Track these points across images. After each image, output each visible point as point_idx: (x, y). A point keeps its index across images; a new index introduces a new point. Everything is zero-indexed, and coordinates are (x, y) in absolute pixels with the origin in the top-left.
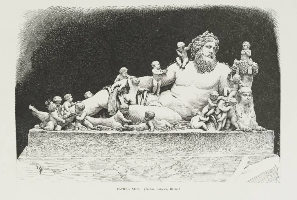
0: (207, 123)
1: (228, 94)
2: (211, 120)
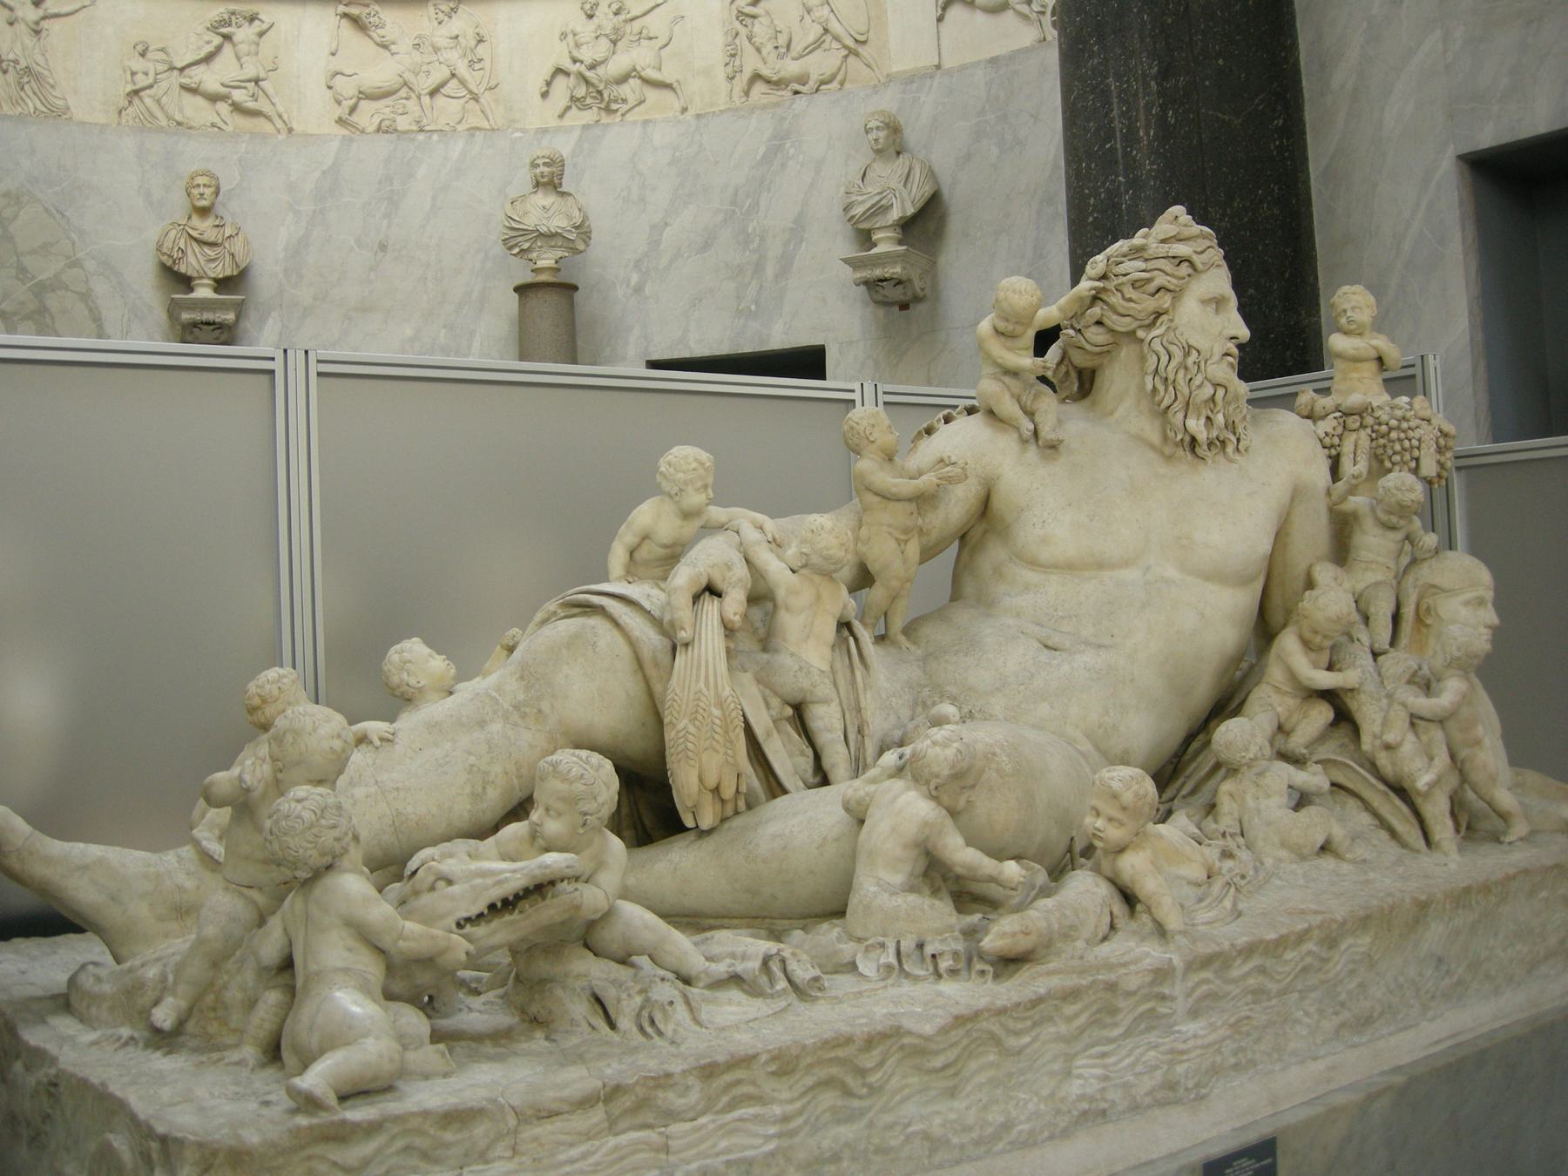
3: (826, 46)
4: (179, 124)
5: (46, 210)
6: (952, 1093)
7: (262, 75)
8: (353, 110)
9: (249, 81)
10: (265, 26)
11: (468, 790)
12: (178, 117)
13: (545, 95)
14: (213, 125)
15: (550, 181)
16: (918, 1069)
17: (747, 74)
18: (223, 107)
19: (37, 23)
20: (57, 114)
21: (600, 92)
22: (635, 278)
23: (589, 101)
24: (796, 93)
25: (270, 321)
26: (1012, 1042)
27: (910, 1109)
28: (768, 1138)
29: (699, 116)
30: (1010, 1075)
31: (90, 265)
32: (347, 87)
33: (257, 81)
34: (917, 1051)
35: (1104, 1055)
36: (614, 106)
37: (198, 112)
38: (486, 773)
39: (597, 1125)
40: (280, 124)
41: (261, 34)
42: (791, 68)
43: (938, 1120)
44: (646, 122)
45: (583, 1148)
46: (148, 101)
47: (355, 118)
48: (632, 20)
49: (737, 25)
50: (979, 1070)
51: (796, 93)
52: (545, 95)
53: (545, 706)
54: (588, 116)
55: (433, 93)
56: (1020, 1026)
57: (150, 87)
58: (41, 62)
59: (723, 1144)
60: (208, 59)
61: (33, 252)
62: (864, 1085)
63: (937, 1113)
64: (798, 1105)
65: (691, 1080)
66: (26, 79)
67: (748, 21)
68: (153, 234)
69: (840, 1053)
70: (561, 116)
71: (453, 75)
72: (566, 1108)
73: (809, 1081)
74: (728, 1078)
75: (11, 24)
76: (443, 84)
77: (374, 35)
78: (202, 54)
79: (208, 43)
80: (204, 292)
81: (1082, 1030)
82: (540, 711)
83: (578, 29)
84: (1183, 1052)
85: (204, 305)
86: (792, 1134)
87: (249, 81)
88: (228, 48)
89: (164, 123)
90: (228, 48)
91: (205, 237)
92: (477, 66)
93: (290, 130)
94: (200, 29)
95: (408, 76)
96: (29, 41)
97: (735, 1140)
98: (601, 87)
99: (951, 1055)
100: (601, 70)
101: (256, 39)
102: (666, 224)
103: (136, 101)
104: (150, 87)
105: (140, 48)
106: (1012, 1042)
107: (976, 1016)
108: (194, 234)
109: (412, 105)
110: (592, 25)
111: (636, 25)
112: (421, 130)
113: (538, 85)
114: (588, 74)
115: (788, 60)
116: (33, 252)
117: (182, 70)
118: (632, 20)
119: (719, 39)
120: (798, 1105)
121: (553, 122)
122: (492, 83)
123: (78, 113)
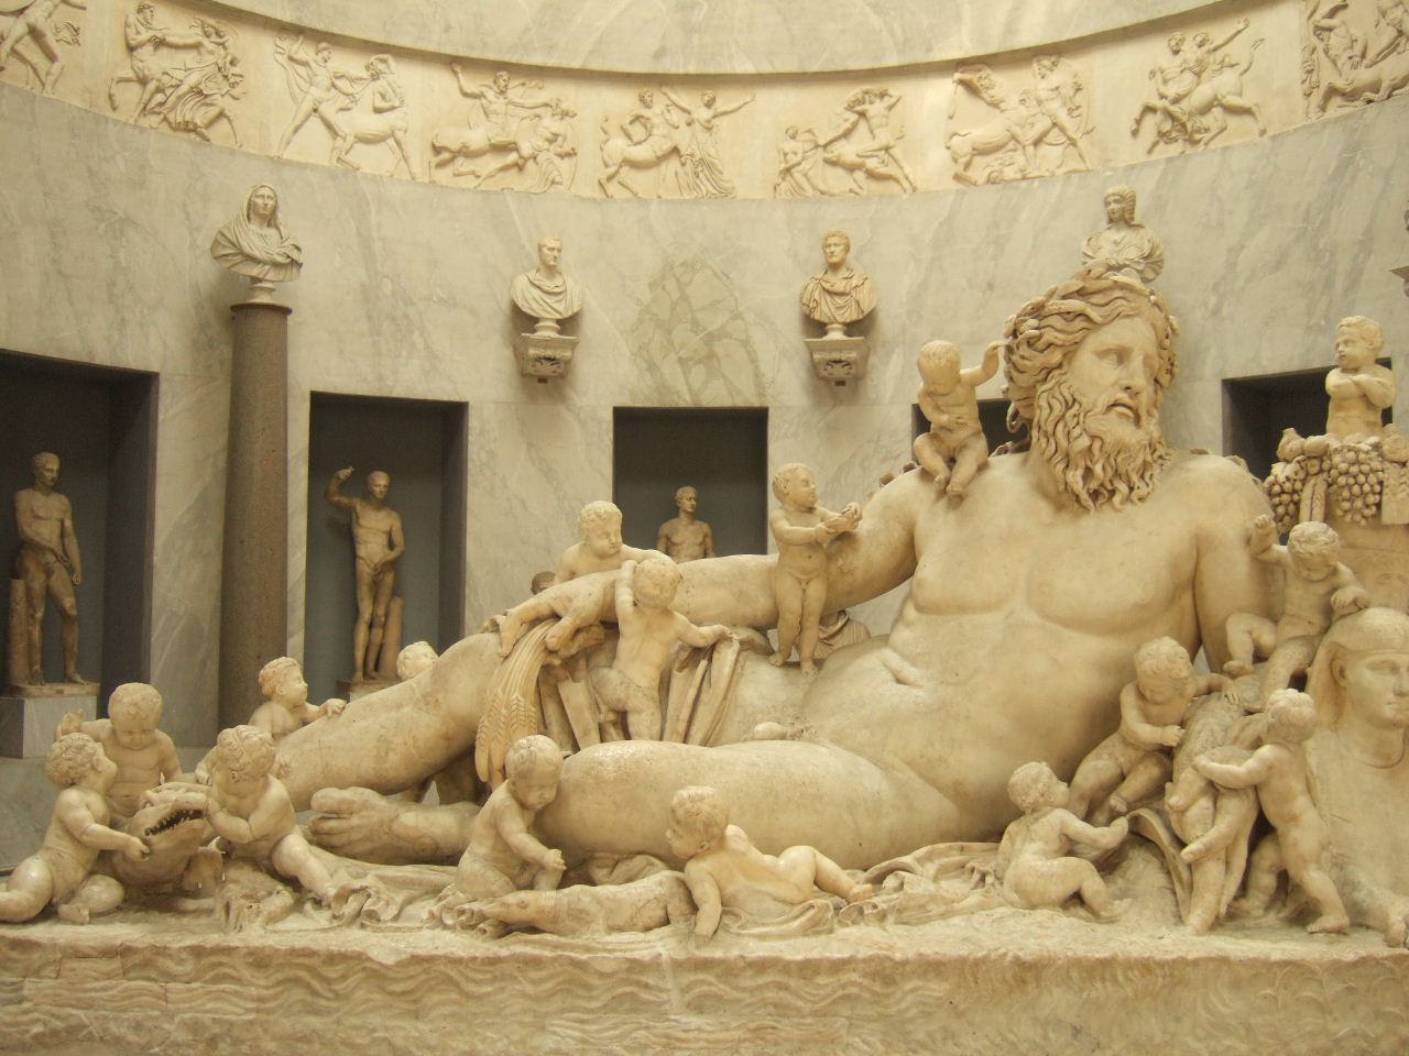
0: (1108, 864)
1: (1260, 656)
2: (1138, 836)
3: (1400, 49)
4: (822, 193)
5: (715, 274)
6: (416, 1016)
7: (892, 143)
8: (967, 166)
9: (880, 150)
10: (893, 100)
11: (374, 753)
12: (822, 187)
13: (1135, 133)
14: (851, 191)
15: (1122, 216)
16: (382, 990)
17: (1323, 88)
18: (860, 175)
19: (708, 121)
20: (724, 194)
21: (1184, 125)
22: (1213, 300)
23: (1174, 134)
24: (1370, 102)
25: (895, 356)
26: (472, 988)
27: (374, 1020)
28: (248, 1011)
29: (1274, 138)
30: (475, 1015)
31: (750, 317)
32: (962, 145)
33: (887, 149)
34: (378, 975)
35: (582, 1022)
36: (1197, 137)
37: (837, 180)
38: (391, 742)
39: (114, 970)
40: (906, 184)
41: (890, 108)
42: (1364, 75)
43: (402, 1033)
44: (1225, 149)
45: (107, 983)
46: (797, 175)
47: (970, 174)
48: (1215, 49)
49: (1315, 41)
50: (443, 1003)
51: (1370, 102)
52: (1135, 133)
53: (440, 697)
54: (1175, 149)
55: (1037, 143)
56: (479, 976)
57: (799, 164)
58: (712, 151)
59: (209, 1006)
60: (847, 134)
61: (703, 309)
62: (330, 990)
63: (401, 1028)
64: (272, 992)
65: (184, 955)
66: (700, 169)
67: (1325, 34)
68: (798, 288)
69: (307, 961)
70: (1150, 152)
71: (1055, 124)
72: (95, 954)
73: (280, 976)
74: (214, 959)
75: (689, 125)
76: (1045, 134)
77: (986, 96)
78: (841, 131)
79: (846, 120)
80: (836, 335)
81: (551, 995)
82: (437, 701)
83: (1165, 66)
84: (683, 1041)
85: (836, 346)
86: (268, 1012)
87: (880, 150)
88: (863, 125)
89: (810, 192)
90: (863, 125)
91: (835, 289)
92: (1075, 113)
93: (914, 189)
94: (840, 109)
95: (1017, 130)
96: (702, 136)
97: (219, 1005)
98: (1184, 119)
99: (410, 985)
100: (1184, 104)
101: (886, 112)
102: (1242, 247)
103: (788, 178)
104: (799, 164)
105: (791, 132)
106: (472, 988)
107: (431, 959)
108: (827, 286)
109: (1019, 159)
110: (1178, 59)
111: (1219, 55)
112: (1024, 178)
113: (1128, 124)
114: (1173, 108)
115: (1362, 69)
116: (703, 309)
117: (825, 146)
118: (1215, 49)
119: (1297, 56)
120: (272, 992)
121: (1143, 158)
122: (1088, 128)
123: (741, 193)
